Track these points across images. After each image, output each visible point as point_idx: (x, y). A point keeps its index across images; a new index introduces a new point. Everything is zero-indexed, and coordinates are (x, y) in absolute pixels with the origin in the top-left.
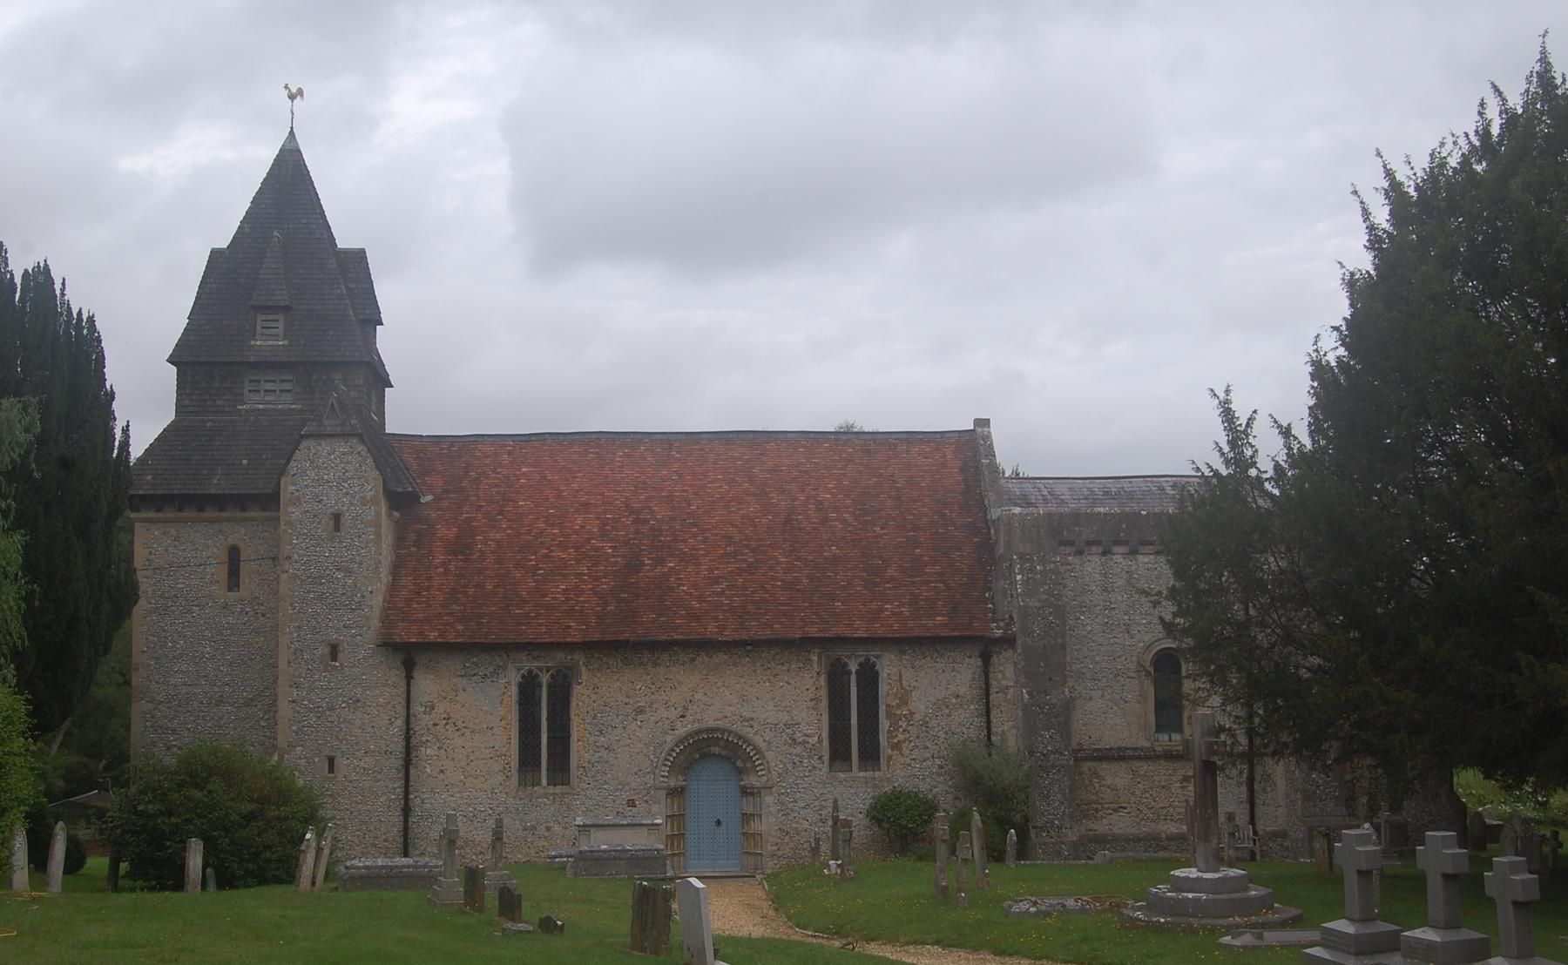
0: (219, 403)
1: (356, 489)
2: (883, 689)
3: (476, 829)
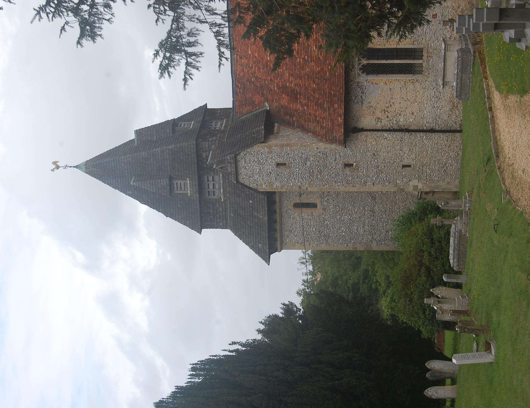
0: (221, 210)
1: (263, 156)
3: (444, 97)
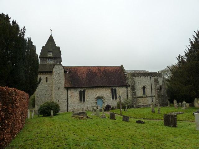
2: (117, 91)
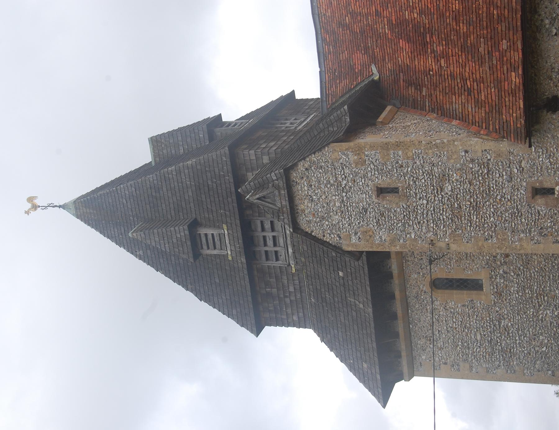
0: (292, 289)
1: (347, 171)
